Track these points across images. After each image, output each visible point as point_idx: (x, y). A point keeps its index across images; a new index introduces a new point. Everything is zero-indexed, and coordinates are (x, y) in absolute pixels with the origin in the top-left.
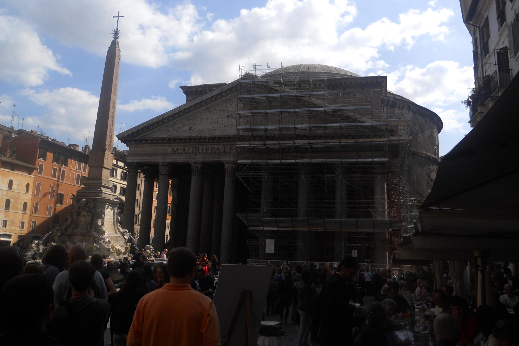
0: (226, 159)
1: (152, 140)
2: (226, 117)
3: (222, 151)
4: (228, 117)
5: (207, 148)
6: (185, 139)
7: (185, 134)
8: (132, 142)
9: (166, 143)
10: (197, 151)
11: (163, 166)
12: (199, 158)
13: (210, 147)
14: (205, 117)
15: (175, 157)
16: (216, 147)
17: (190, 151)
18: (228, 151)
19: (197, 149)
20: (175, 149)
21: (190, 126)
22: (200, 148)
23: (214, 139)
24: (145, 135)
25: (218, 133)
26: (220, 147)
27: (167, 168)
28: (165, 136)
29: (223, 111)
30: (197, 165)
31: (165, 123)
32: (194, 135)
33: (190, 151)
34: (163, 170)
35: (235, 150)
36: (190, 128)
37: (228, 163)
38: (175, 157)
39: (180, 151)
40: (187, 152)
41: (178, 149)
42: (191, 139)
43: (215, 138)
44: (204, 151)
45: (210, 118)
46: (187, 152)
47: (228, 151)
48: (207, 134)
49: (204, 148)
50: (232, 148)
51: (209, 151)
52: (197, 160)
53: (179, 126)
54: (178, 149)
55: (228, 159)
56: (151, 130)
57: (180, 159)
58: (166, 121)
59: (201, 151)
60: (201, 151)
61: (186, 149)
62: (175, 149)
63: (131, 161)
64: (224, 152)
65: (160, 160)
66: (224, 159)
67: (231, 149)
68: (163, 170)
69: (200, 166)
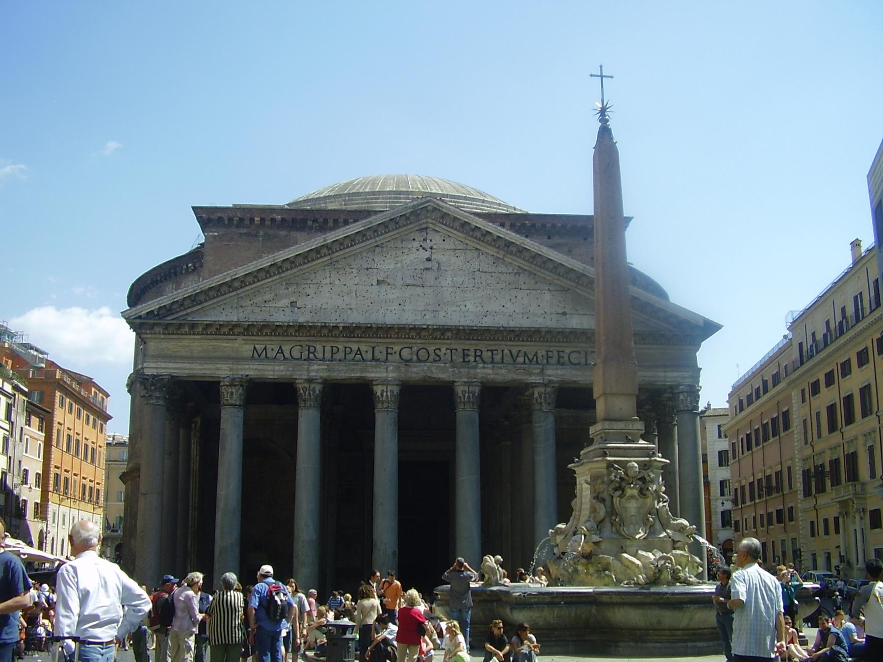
0: (378, 375)
1: (208, 326)
2: (375, 283)
3: (369, 356)
4: (379, 283)
5: (335, 350)
6: (289, 326)
7: (281, 318)
8: (157, 329)
9: (238, 335)
10: (311, 356)
11: (232, 385)
12: (318, 371)
13: (341, 347)
14: (328, 281)
15: (260, 367)
16: (355, 347)
17: (296, 354)
18: (382, 357)
19: (312, 349)
20: (260, 347)
21: (293, 299)
22: (319, 348)
23: (352, 331)
24: (187, 314)
25: (356, 318)
26: (363, 348)
27: (241, 391)
28: (235, 319)
29: (367, 269)
30: (312, 386)
31: (236, 289)
32: (302, 320)
33: (296, 354)
34: (232, 396)
35: (397, 356)
36: (293, 304)
37: (385, 382)
38: (260, 367)
39: (270, 354)
40: (287, 355)
41: (265, 348)
42: (301, 328)
43: (358, 327)
44: (328, 355)
45: (337, 282)
46: (287, 355)
47: (382, 357)
48: (332, 319)
49: (328, 349)
50: (390, 351)
51: (341, 355)
52: (314, 374)
53: (267, 297)
54: (265, 348)
55: (385, 375)
56: (201, 303)
57: (273, 371)
58: (237, 284)
59: (320, 355)
60: (320, 355)
61: (286, 348)
62: (260, 347)
63: (154, 372)
64: (373, 359)
65: (223, 371)
66: (373, 373)
67: (387, 354)
68: (232, 396)
69: (318, 388)
